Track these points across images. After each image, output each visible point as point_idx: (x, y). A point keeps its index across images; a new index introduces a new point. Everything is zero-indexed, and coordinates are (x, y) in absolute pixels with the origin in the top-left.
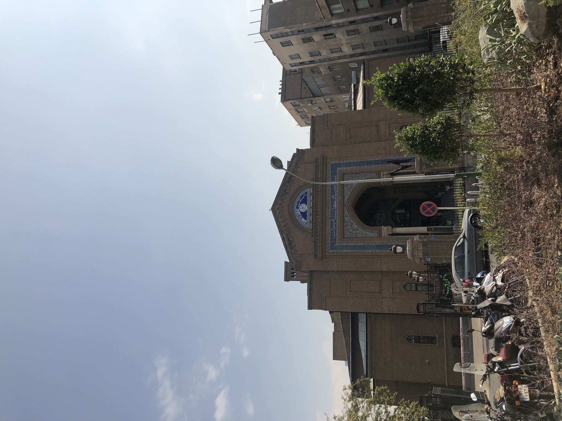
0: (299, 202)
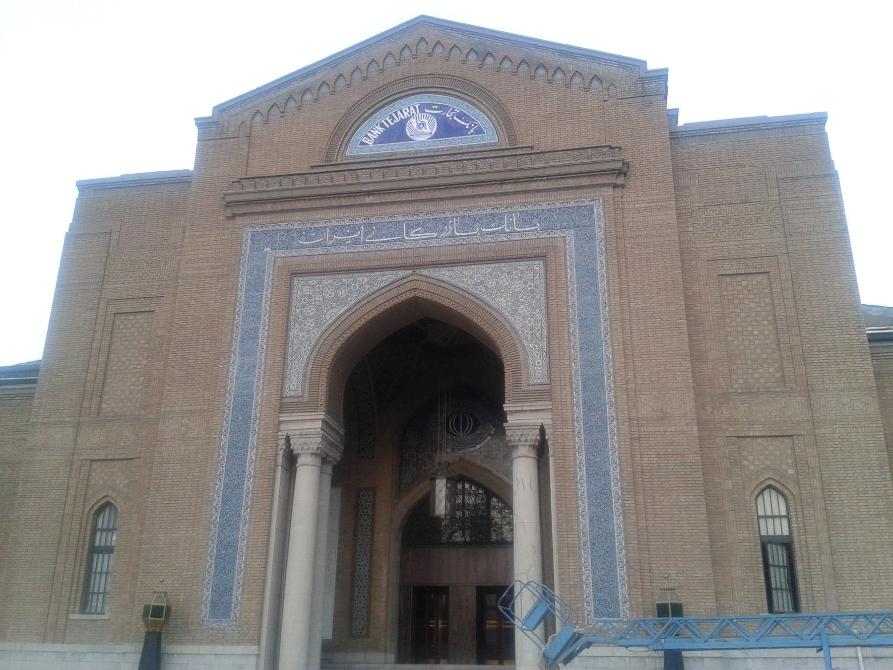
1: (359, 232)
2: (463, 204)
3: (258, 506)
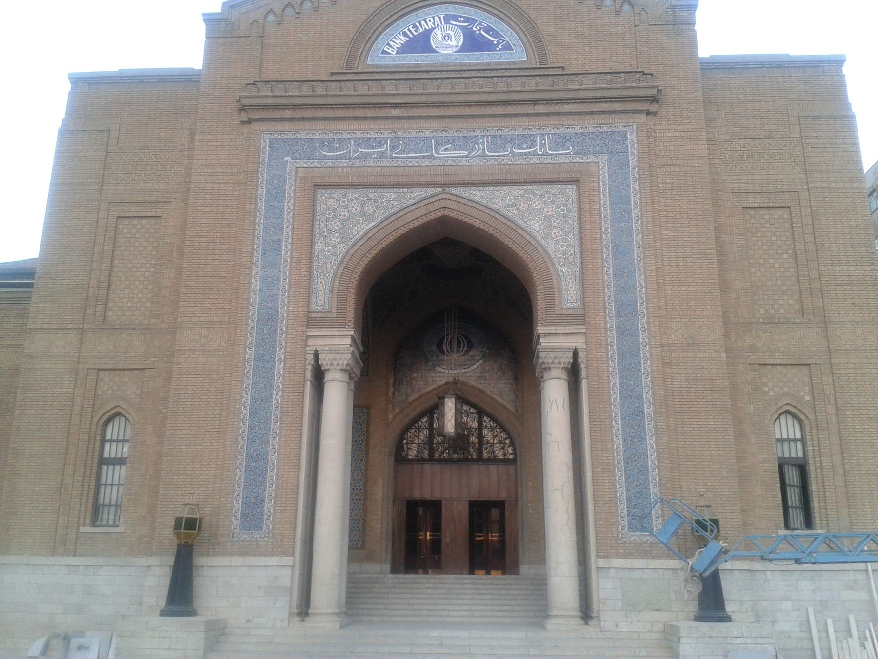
0: (474, 21)
1: (385, 146)
2: (493, 123)
3: (288, 420)
